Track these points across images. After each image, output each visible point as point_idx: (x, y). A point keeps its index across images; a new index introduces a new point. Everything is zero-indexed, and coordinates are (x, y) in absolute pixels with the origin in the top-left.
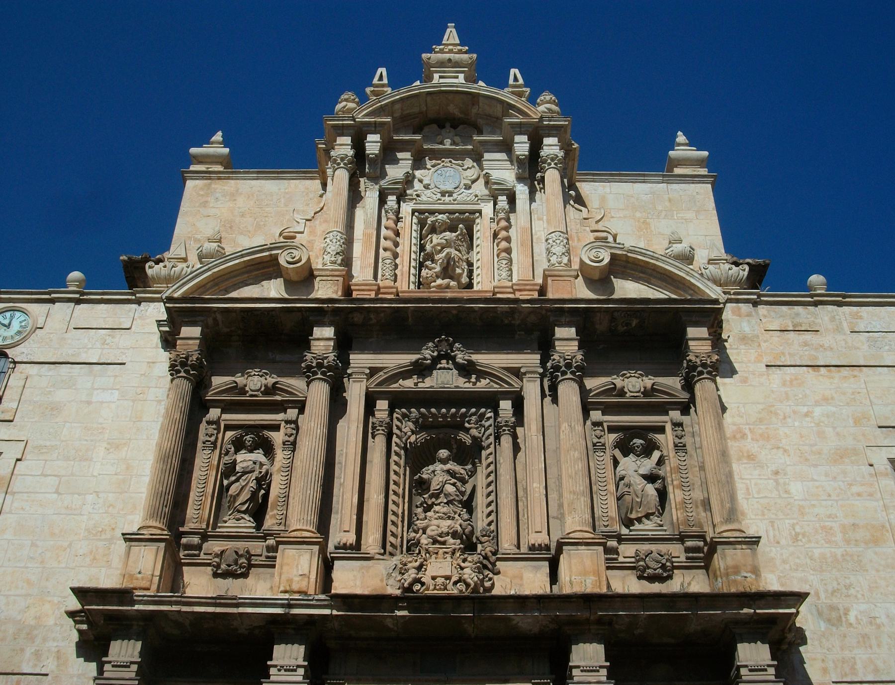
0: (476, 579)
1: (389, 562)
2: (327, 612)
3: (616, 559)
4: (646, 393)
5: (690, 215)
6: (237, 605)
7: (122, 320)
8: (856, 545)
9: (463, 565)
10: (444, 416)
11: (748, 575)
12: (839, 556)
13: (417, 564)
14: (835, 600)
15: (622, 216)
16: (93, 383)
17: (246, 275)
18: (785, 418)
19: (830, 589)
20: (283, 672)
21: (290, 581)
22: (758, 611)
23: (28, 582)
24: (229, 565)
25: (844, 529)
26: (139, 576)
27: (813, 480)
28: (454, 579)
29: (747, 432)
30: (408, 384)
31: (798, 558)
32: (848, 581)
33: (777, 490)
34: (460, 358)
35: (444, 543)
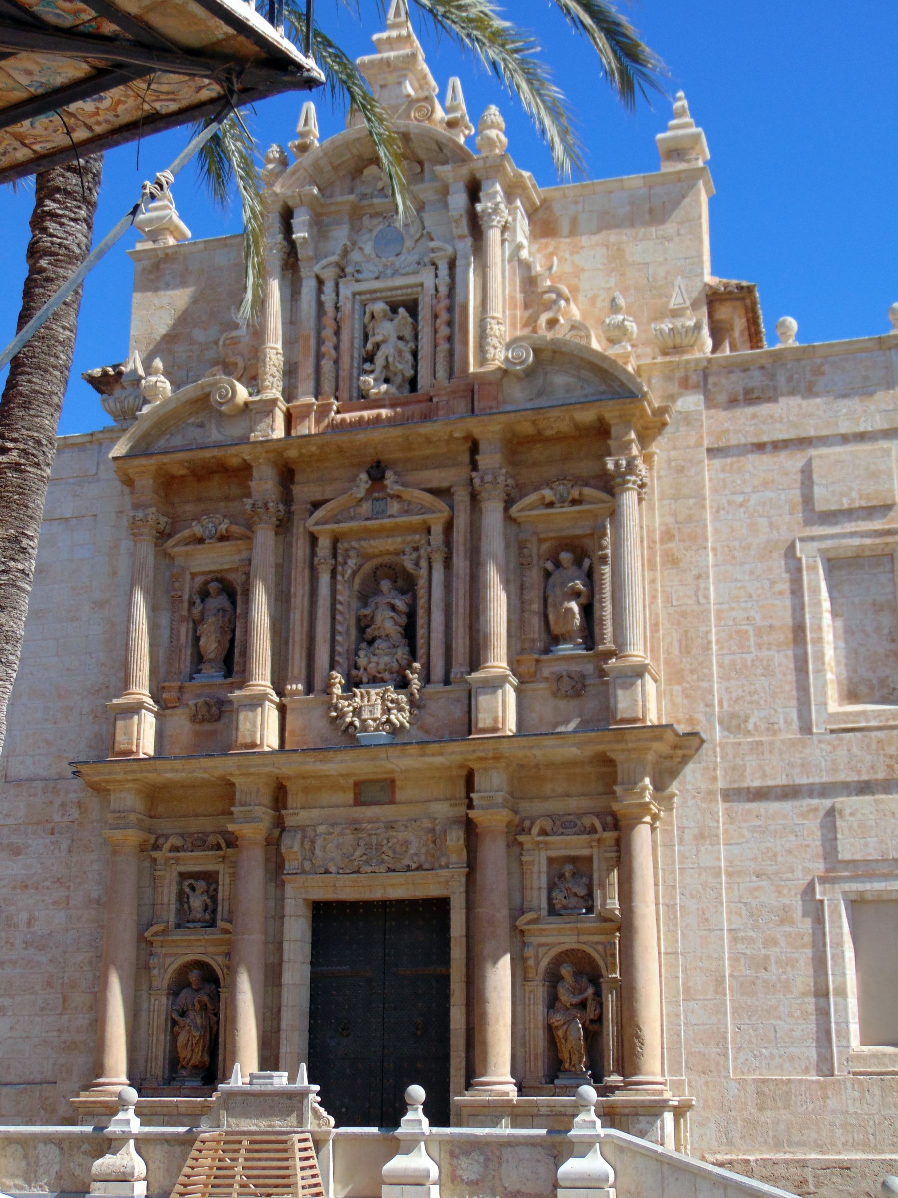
8: (769, 649)
12: (749, 663)
14: (737, 708)
19: (734, 696)
23: (47, 741)
25: (759, 632)
27: (737, 580)
29: (676, 532)
32: (753, 687)
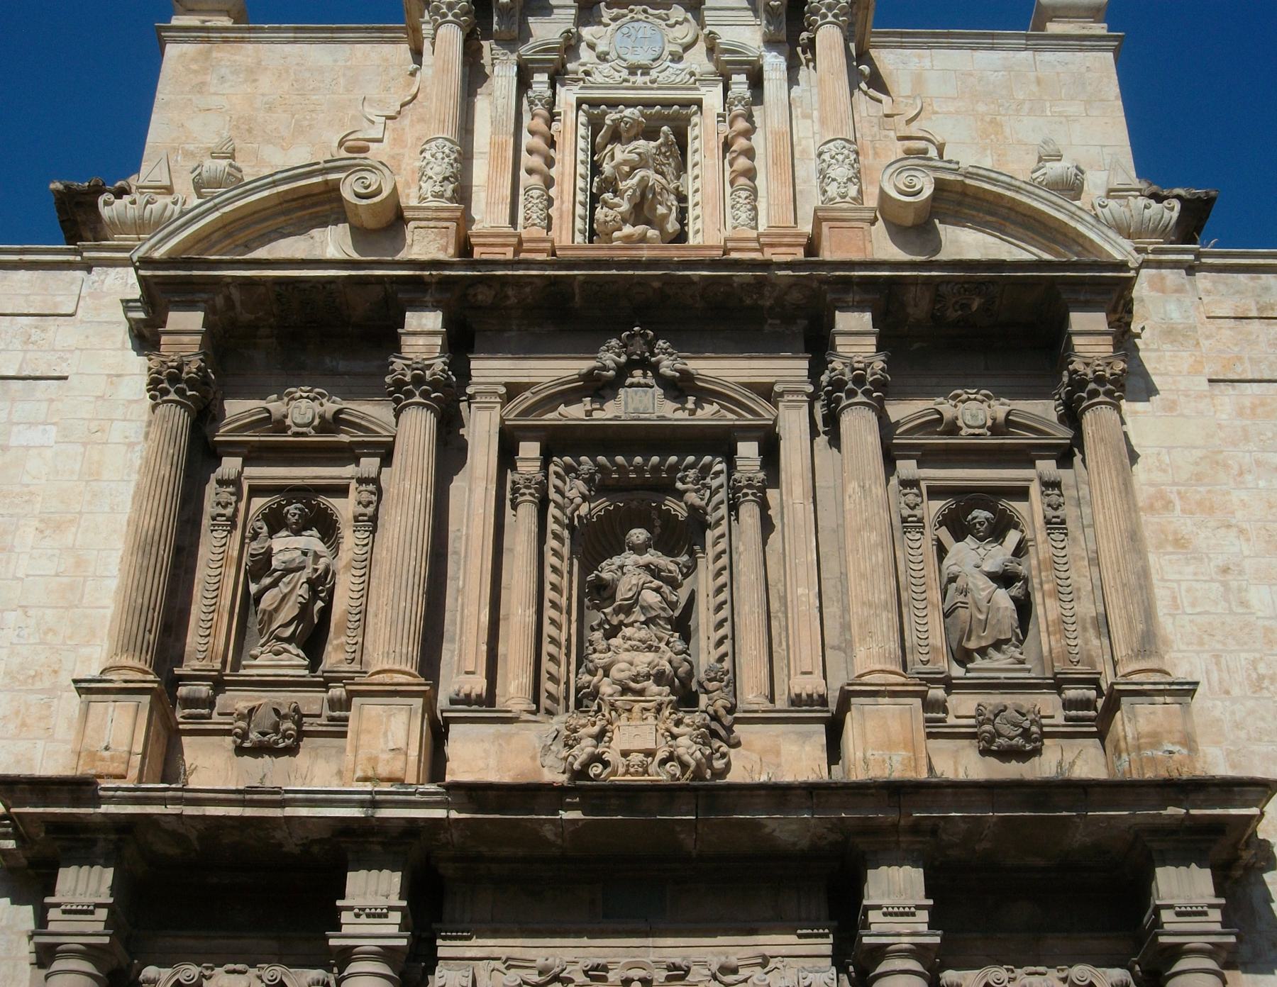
0: (698, 754)
1: (547, 726)
2: (440, 813)
3: (943, 720)
4: (996, 429)
5: (1074, 108)
6: (282, 804)
7: (58, 299)
9: (675, 730)
10: (639, 469)
11: (1176, 748)
13: (596, 729)
15: (952, 110)
16: (10, 413)
17: (283, 218)
18: (1241, 474)
20: (363, 919)
21: (373, 760)
22: (1193, 812)
24: (264, 734)
26: (107, 754)
28: (661, 755)
29: (1174, 497)
30: (575, 413)
31: (1263, 719)
33: (1227, 601)
34: (668, 366)
35: (641, 692)
